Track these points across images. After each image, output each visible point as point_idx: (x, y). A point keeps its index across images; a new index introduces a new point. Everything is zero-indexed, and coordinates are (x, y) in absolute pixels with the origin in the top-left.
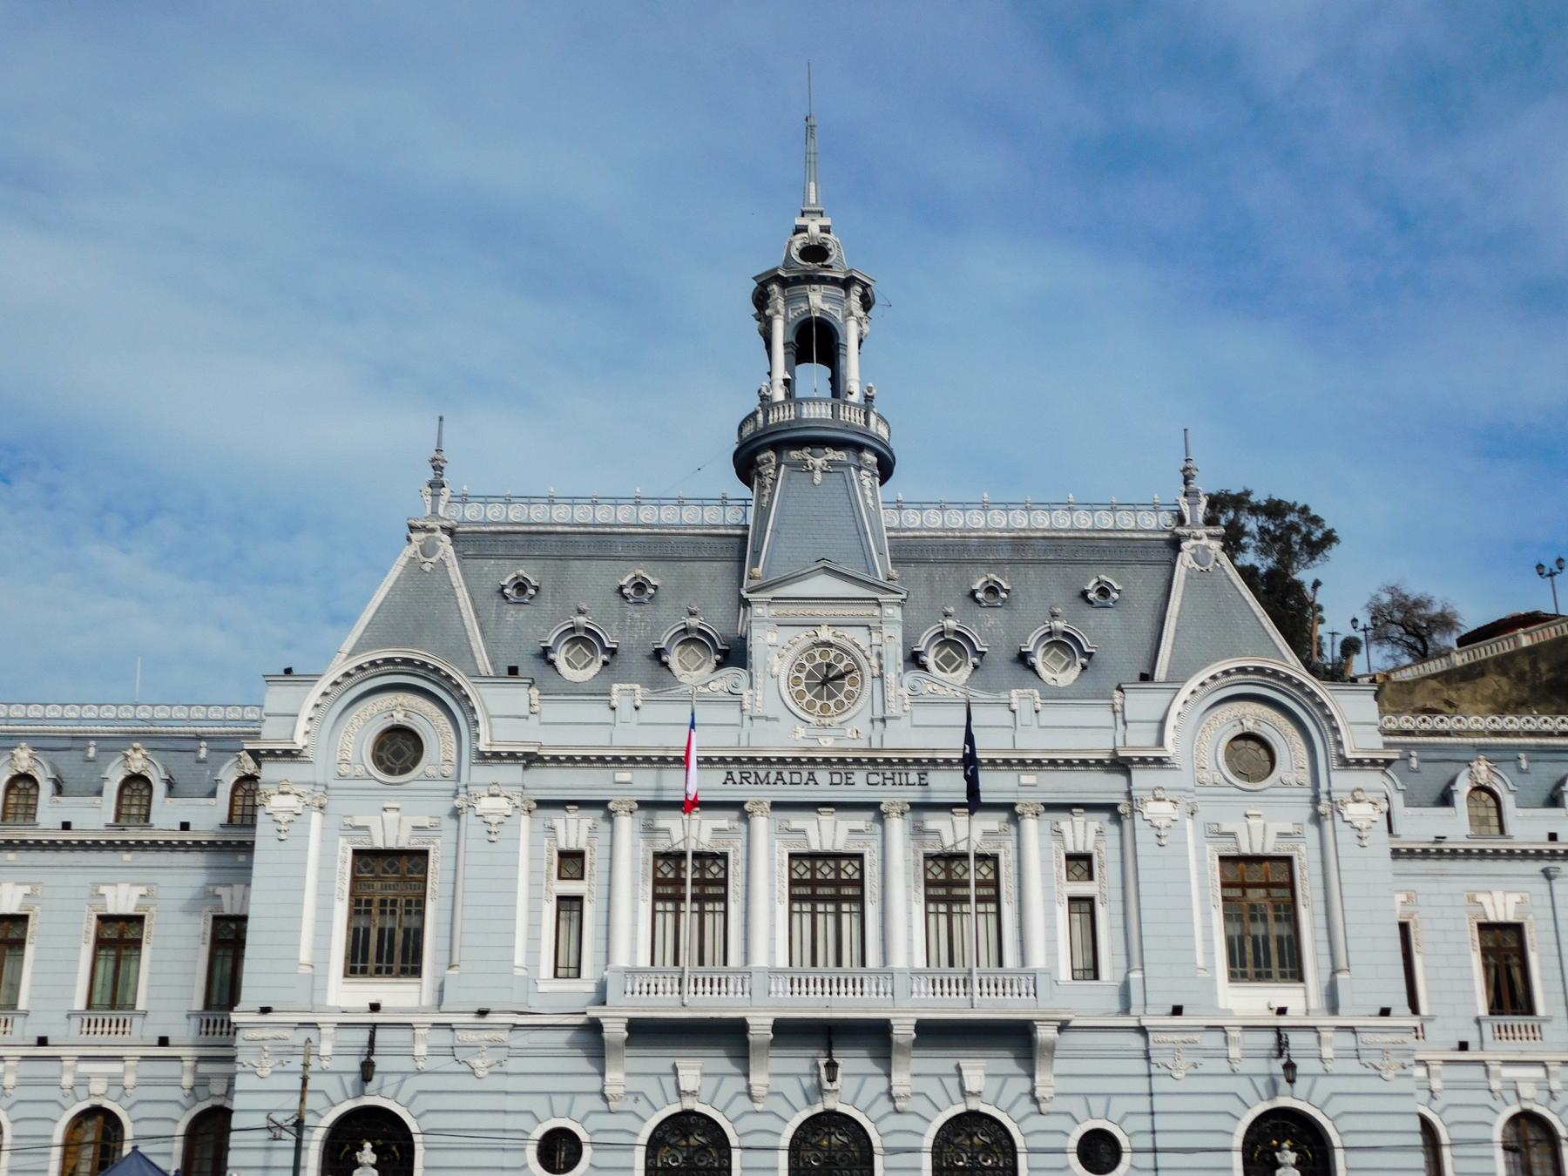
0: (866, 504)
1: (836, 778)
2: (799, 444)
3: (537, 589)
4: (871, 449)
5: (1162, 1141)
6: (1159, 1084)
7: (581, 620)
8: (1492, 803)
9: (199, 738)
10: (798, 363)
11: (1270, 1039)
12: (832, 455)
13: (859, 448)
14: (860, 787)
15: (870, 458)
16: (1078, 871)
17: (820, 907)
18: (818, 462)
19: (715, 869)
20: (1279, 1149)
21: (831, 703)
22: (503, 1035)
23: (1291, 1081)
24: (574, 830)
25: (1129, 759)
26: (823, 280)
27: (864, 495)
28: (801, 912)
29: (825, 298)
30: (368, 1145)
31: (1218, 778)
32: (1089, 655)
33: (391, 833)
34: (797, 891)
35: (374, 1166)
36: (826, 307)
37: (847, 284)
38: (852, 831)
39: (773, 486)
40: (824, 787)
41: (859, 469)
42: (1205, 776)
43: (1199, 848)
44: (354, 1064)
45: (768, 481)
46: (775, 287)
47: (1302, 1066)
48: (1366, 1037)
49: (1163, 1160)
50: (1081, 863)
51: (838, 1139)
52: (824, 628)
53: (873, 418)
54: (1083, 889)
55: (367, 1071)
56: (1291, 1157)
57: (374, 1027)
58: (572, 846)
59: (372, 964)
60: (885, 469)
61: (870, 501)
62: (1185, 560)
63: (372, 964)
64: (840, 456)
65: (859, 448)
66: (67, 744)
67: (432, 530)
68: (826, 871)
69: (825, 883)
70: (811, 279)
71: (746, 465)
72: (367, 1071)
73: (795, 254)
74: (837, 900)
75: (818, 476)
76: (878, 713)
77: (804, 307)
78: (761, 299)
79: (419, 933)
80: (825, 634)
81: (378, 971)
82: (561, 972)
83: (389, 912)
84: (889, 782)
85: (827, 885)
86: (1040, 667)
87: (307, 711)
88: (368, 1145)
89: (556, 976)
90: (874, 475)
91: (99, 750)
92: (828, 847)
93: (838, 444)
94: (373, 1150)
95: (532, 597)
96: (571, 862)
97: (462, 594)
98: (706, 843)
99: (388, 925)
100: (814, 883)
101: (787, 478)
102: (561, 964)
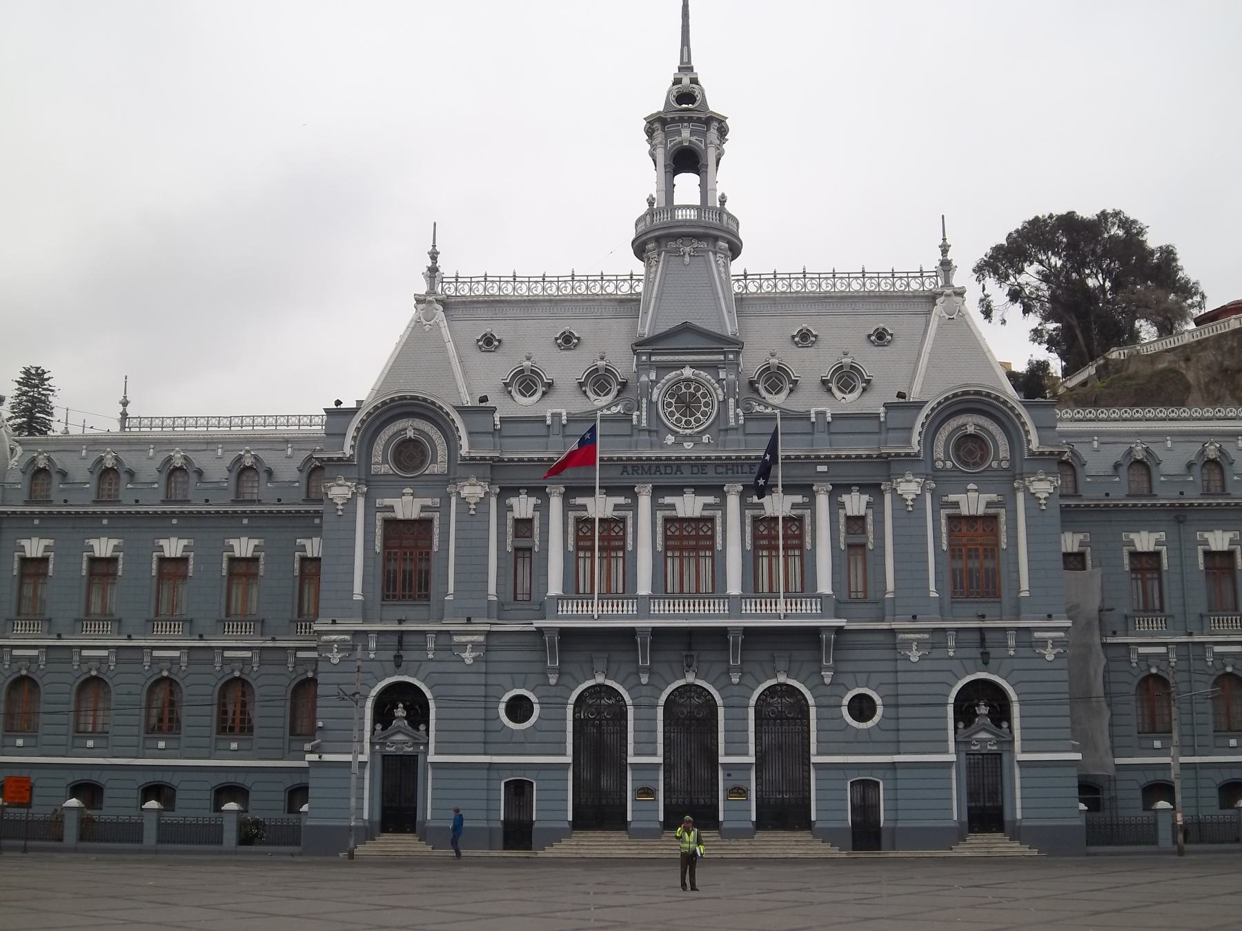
1: (695, 470)
2: (675, 237)
3: (500, 341)
4: (724, 239)
5: (901, 700)
6: (901, 665)
7: (528, 363)
8: (1144, 472)
9: (287, 441)
10: (676, 173)
11: (977, 636)
14: (710, 478)
15: (724, 245)
16: (856, 528)
17: (685, 554)
18: (687, 249)
19: (617, 530)
20: (978, 705)
21: (692, 419)
22: (481, 638)
23: (986, 663)
24: (523, 506)
25: (889, 455)
26: (690, 120)
28: (673, 557)
30: (401, 705)
32: (868, 382)
33: (407, 507)
34: (670, 543)
35: (406, 718)
36: (693, 139)
38: (705, 505)
39: (657, 266)
40: (686, 477)
42: (939, 465)
44: (390, 655)
45: (653, 263)
46: (657, 125)
47: (994, 652)
48: (1037, 635)
49: (903, 712)
50: (856, 522)
51: (696, 701)
52: (688, 368)
53: (725, 217)
54: (856, 540)
55: (398, 661)
56: (983, 710)
57: (401, 633)
58: (523, 516)
59: (399, 592)
60: (735, 250)
62: (938, 309)
63: (399, 592)
64: (703, 245)
65: (716, 239)
66: (204, 447)
67: (430, 302)
68: (689, 530)
69: (689, 537)
70: (682, 120)
71: (640, 249)
72: (398, 661)
73: (672, 98)
74: (696, 549)
75: (687, 259)
76: (722, 427)
77: (678, 139)
78: (650, 132)
79: (428, 572)
80: (688, 372)
81: (404, 597)
82: (520, 597)
83: (407, 559)
85: (689, 540)
86: (835, 390)
87: (351, 432)
88: (401, 705)
89: (515, 599)
90: (726, 257)
91: (224, 451)
92: (689, 514)
93: (699, 237)
94: (405, 708)
95: (497, 347)
96: (523, 525)
97: (450, 346)
98: (609, 513)
99: (408, 568)
100: (681, 538)
101: (666, 262)
102: (519, 591)
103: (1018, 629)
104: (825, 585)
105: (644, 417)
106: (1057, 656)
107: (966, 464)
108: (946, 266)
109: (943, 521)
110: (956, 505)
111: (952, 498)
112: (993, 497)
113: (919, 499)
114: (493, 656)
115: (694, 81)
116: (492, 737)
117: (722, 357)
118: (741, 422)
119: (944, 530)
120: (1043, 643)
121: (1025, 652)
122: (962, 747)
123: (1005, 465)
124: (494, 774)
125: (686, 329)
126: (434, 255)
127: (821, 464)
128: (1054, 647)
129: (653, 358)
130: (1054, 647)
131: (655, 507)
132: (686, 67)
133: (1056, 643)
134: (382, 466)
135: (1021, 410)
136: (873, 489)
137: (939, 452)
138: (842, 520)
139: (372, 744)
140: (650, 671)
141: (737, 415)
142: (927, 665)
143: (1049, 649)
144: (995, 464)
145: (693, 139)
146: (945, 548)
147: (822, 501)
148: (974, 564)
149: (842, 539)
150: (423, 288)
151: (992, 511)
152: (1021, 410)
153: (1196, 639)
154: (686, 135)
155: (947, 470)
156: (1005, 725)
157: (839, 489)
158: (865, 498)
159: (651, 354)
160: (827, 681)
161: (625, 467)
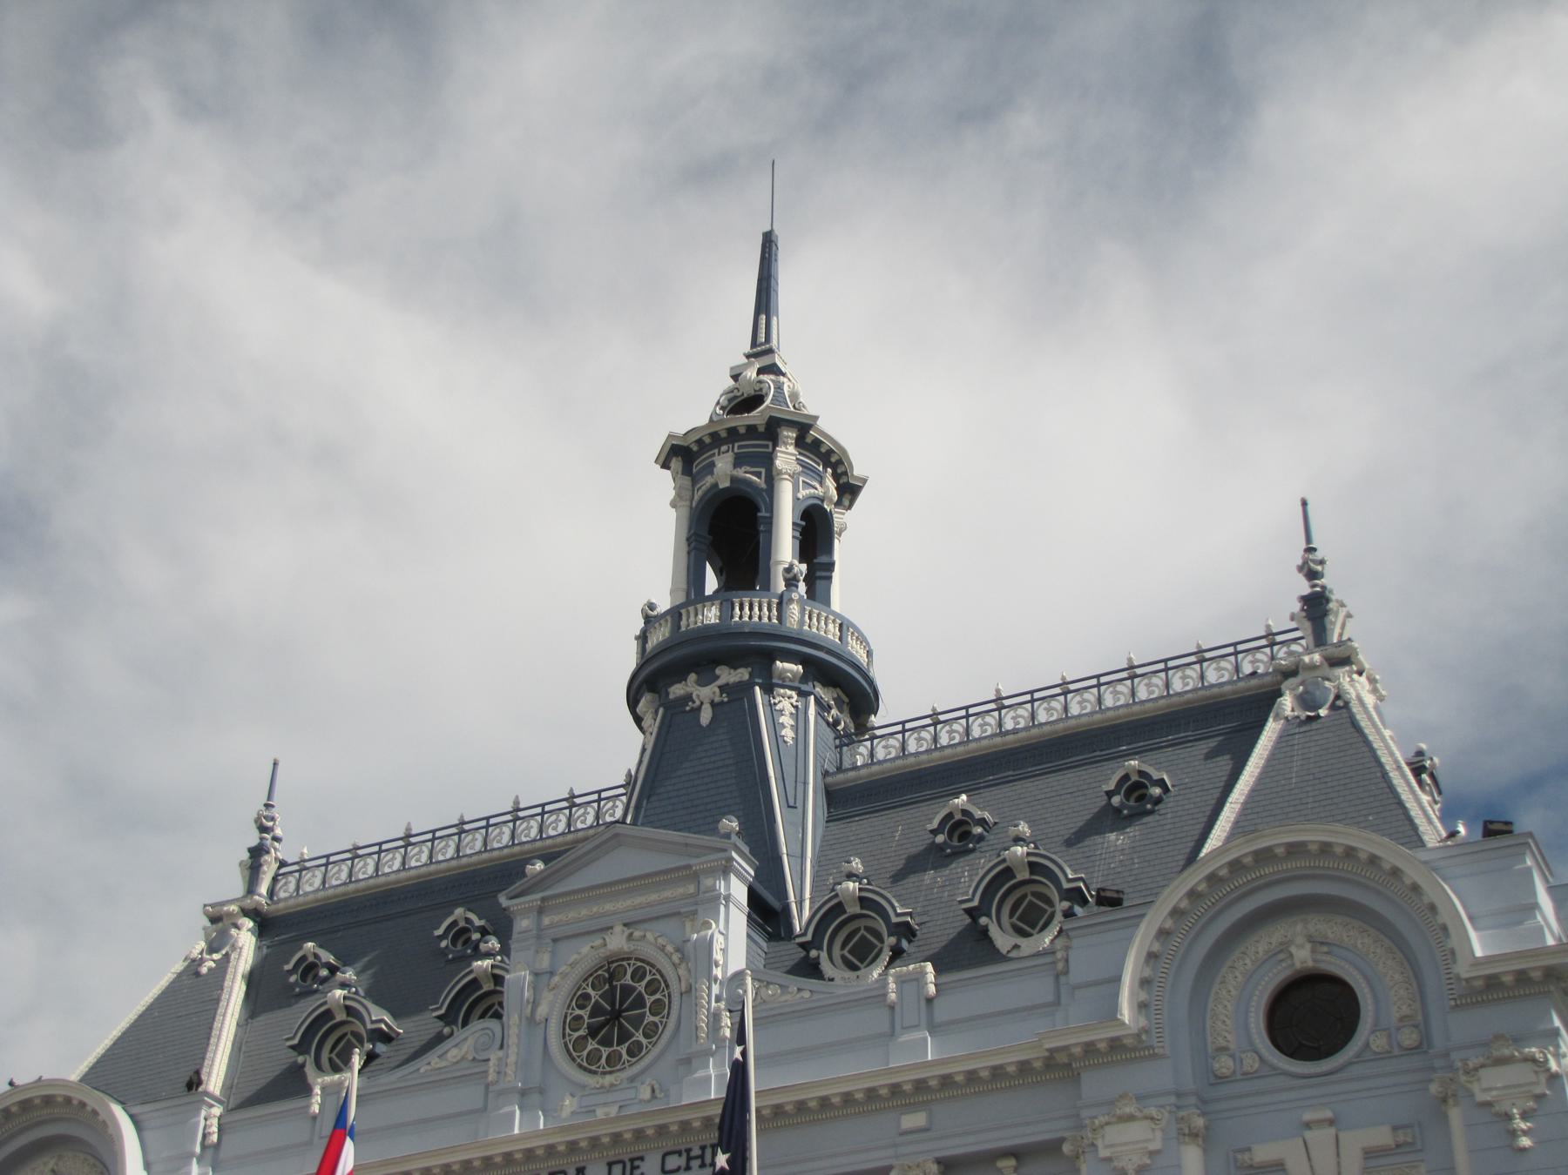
0: (777, 738)
12: (726, 675)
27: (775, 727)
29: (739, 461)
31: (1251, 1063)
36: (740, 473)
37: (773, 428)
41: (769, 690)
46: (676, 463)
61: (788, 734)
64: (743, 674)
65: (770, 656)
77: (709, 480)
80: (617, 941)
84: (695, 1164)
86: (994, 932)
93: (733, 658)
105: (512, 1059)
108: (1316, 607)
112: (1381, 1136)
115: (773, 369)
117: (691, 889)
123: (1408, 1038)
127: (912, 1107)
129: (546, 921)
132: (761, 349)
145: (740, 473)
150: (236, 887)
154: (724, 468)
155: (1248, 1076)
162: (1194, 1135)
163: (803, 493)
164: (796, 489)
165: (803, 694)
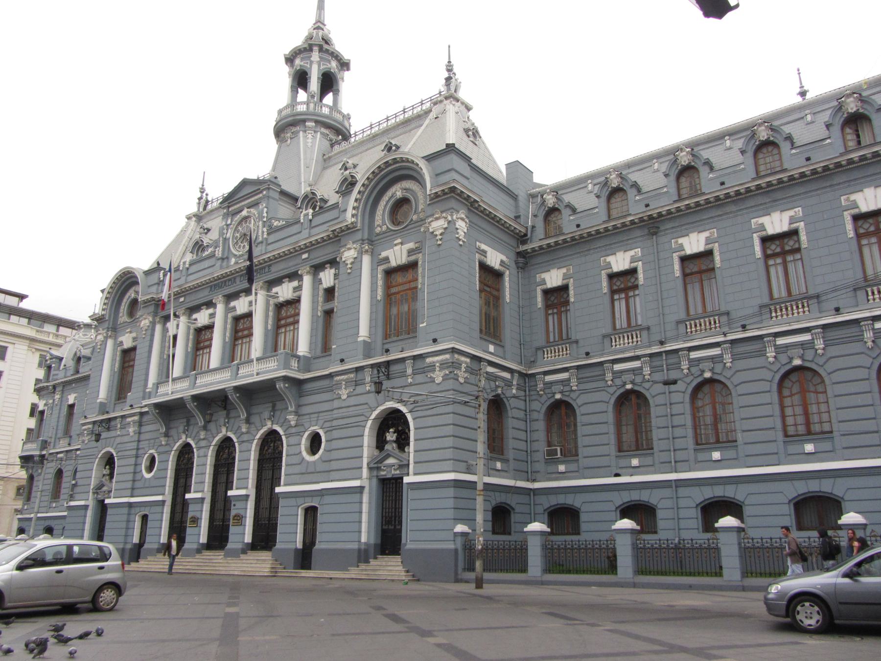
6: (336, 404)
12: (294, 129)
13: (304, 121)
18: (289, 135)
29: (302, 59)
36: (302, 63)
43: (373, 271)
48: (429, 360)
50: (330, 292)
65: (304, 121)
75: (289, 141)
80: (244, 213)
103: (415, 358)
104: (303, 348)
106: (445, 378)
107: (399, 224)
109: (379, 276)
110: (387, 259)
111: (384, 254)
112: (411, 245)
113: (357, 261)
114: (144, 429)
116: (137, 484)
118: (265, 236)
119: (380, 283)
120: (432, 367)
121: (420, 378)
122: (375, 473)
124: (133, 511)
125: (245, 183)
126: (202, 190)
128: (441, 369)
130: (441, 369)
131: (228, 310)
133: (443, 365)
134: (123, 317)
135: (422, 164)
136: (333, 263)
137: (378, 220)
138: (321, 293)
139: (94, 493)
140: (205, 428)
141: (263, 232)
142: (353, 401)
143: (437, 372)
144: (415, 217)
146: (379, 298)
147: (307, 280)
148: (405, 308)
149: (320, 308)
151: (413, 258)
152: (422, 164)
153: (668, 347)
156: (406, 450)
157: (317, 268)
158: (333, 271)
159: (229, 207)
160: (293, 423)
161: (211, 287)
162: (367, 251)
163: (322, 67)
164: (319, 66)
165: (315, 132)
